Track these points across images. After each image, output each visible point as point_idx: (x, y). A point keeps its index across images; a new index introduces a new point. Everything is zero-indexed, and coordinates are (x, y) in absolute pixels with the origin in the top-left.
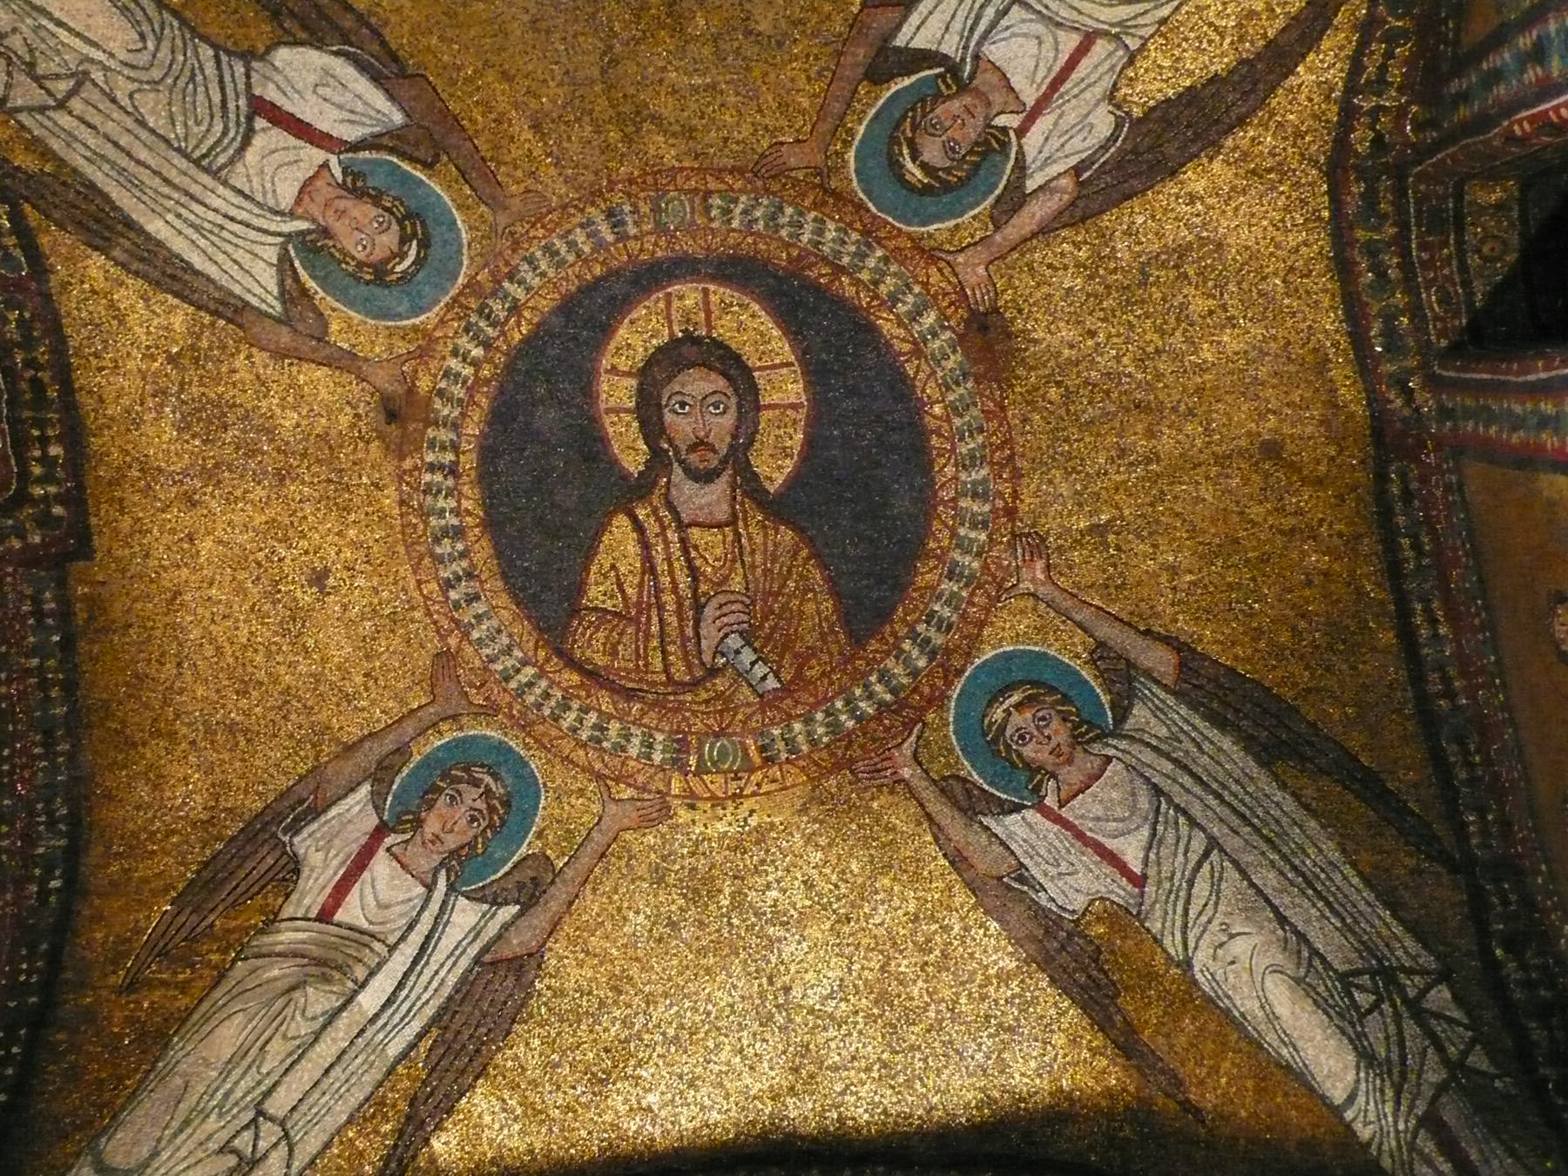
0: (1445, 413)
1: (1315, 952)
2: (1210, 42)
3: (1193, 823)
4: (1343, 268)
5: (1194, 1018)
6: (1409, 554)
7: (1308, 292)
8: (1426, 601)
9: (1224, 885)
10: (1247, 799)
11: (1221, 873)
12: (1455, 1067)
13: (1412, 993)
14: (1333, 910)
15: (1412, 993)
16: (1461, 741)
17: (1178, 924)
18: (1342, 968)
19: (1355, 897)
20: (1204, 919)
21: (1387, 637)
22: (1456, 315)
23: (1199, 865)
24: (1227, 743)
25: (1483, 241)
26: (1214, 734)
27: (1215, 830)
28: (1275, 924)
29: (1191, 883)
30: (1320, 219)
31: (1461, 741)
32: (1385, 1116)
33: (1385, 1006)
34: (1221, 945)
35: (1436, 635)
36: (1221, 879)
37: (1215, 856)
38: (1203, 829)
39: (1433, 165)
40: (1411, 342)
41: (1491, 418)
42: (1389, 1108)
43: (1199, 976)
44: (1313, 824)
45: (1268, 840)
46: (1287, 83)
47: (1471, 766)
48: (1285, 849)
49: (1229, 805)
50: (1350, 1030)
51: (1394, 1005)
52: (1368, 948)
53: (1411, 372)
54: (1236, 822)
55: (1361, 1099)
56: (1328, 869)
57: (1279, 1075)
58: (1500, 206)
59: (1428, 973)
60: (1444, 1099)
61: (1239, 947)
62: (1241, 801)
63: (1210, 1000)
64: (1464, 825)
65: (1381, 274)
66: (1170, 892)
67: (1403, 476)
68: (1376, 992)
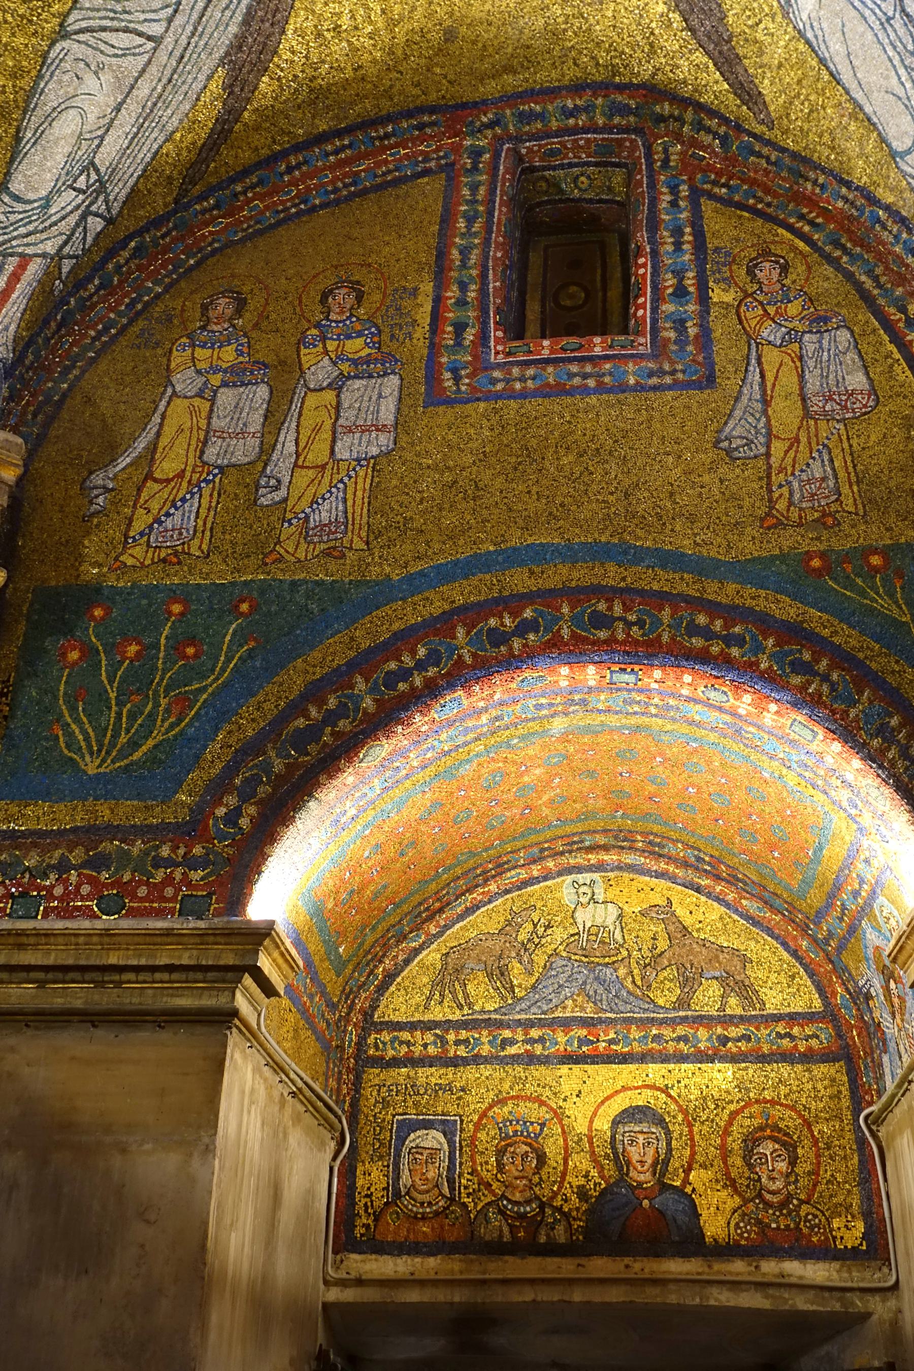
0: (476, 153)
1: (102, 138)
2: (749, 17)
3: (170, 20)
4: (577, 88)
5: (26, 45)
6: (382, 132)
7: (563, 63)
8: (350, 146)
9: (130, 58)
10: (195, 56)
11: (140, 54)
12: (59, 256)
13: (94, 208)
14: (133, 138)
15: (94, 208)
16: (260, 182)
17: (91, 23)
18: (97, 161)
19: (145, 149)
20: (102, 47)
21: (323, 126)
22: (541, 160)
23: (140, 34)
24: (233, 29)
25: (589, 177)
26: (239, 18)
27: (169, 40)
28: (113, 104)
29: (126, 30)
30: (614, 75)
31: (260, 182)
32: (16, 229)
33: (81, 197)
34: (88, 65)
35: (327, 155)
36: (134, 55)
37: (150, 45)
38: (166, 31)
39: (640, 157)
40: (527, 128)
41: (470, 221)
42: (22, 230)
43: (58, 47)
44: (188, 107)
45: (170, 81)
46: (711, 65)
47: (244, 193)
48: (166, 94)
49: (189, 43)
50: (60, 184)
51: (84, 202)
52: (114, 170)
53: (505, 129)
54: (177, 53)
55: (19, 207)
56: (160, 126)
57: (12, 131)
58: (610, 189)
59: (109, 212)
60: (39, 260)
61: (91, 82)
62: (193, 52)
63: (45, 56)
64: (206, 199)
65: (571, 114)
66: (115, 12)
67: (433, 124)
68: (88, 188)
